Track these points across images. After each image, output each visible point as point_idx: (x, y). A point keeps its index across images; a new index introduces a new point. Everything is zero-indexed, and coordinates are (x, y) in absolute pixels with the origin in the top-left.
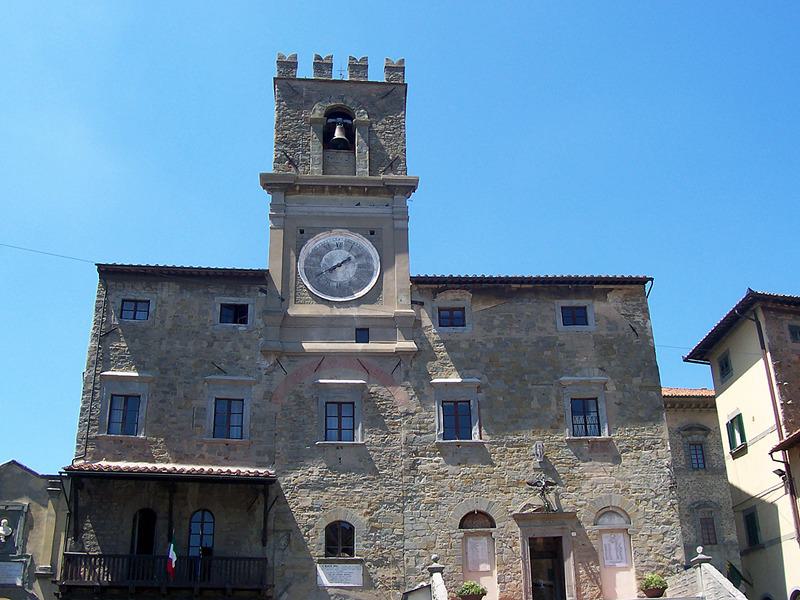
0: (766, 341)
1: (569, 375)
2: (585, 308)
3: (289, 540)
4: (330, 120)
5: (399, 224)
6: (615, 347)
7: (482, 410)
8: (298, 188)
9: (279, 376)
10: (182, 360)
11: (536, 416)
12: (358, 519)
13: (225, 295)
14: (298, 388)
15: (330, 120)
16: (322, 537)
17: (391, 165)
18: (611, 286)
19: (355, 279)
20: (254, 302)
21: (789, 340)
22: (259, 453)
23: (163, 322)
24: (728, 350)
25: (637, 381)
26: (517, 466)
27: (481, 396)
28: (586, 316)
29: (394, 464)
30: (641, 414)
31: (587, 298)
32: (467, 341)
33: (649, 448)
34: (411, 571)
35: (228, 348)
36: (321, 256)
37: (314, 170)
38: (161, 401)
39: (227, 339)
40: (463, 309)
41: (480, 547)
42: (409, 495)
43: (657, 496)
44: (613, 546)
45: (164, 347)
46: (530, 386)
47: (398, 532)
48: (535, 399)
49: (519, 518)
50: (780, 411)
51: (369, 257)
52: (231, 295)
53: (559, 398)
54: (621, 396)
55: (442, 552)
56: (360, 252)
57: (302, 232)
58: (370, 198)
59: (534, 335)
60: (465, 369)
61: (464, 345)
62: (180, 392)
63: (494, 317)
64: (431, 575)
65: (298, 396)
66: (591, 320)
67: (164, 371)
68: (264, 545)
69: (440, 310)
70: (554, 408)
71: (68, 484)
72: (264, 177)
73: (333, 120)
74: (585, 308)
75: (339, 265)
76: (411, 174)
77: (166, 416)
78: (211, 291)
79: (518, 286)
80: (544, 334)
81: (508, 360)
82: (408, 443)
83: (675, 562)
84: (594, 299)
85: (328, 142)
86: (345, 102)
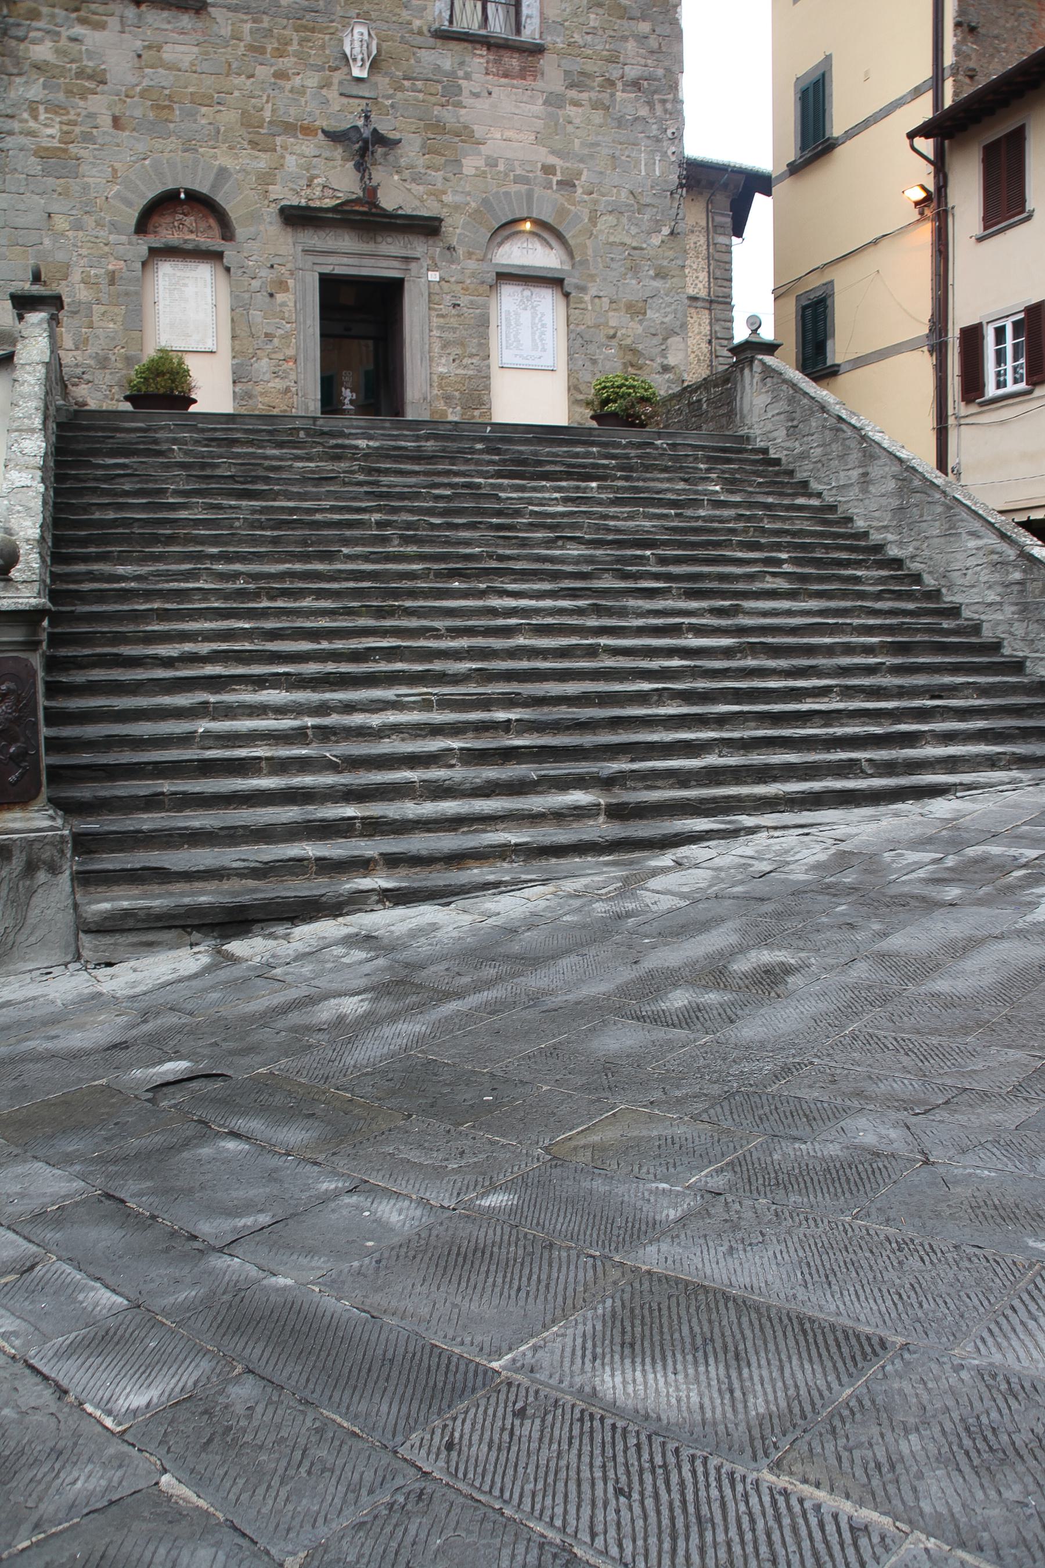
26: (297, 81)
33: (635, 85)
43: (642, 207)
49: (297, 218)
50: (950, 40)
64: (21, 318)
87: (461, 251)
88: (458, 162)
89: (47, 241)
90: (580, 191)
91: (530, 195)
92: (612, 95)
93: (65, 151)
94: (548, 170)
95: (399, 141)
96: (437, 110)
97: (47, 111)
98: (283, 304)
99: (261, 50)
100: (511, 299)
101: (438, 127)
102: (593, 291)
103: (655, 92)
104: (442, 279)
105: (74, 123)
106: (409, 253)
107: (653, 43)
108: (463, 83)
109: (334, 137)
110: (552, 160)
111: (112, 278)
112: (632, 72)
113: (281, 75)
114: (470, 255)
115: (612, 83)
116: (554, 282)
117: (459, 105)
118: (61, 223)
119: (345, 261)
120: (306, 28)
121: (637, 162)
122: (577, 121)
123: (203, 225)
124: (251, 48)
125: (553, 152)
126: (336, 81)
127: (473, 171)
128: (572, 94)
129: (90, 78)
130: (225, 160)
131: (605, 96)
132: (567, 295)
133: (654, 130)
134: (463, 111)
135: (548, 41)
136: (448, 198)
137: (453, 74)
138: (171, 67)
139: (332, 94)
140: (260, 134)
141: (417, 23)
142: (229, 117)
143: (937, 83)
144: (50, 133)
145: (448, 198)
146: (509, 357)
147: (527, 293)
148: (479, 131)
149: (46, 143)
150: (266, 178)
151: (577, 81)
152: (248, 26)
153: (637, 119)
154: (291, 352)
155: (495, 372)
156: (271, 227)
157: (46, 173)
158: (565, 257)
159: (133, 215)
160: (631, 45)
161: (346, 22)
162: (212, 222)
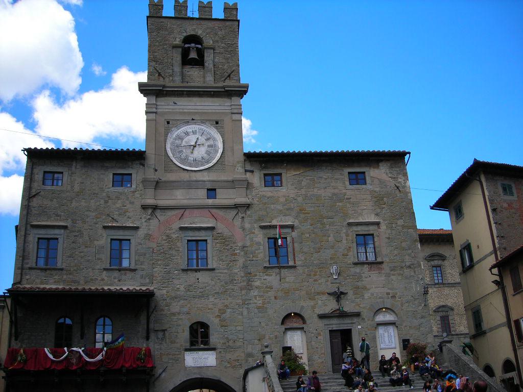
0: (487, 193)
2: (364, 173)
3: (164, 334)
4: (187, 46)
5: (235, 117)
7: (296, 245)
8: (165, 92)
9: (154, 222)
10: (86, 213)
11: (332, 247)
12: (213, 321)
13: (112, 167)
14: (168, 231)
15: (187, 46)
16: (184, 335)
17: (229, 76)
18: (382, 158)
19: (206, 155)
21: (502, 195)
22: (142, 277)
23: (72, 187)
24: (461, 201)
25: (400, 222)
27: (294, 234)
28: (365, 179)
29: (235, 282)
31: (366, 166)
32: (284, 196)
33: (409, 267)
34: (250, 355)
35: (119, 204)
36: (182, 139)
37: (175, 82)
39: (118, 198)
41: (295, 338)
42: (246, 303)
43: (415, 300)
44: (386, 335)
46: (327, 226)
47: (239, 328)
48: (331, 235)
49: (322, 317)
51: (214, 140)
52: (120, 168)
53: (347, 235)
56: (209, 136)
57: (168, 123)
59: (329, 192)
60: (283, 216)
61: (282, 200)
66: (367, 178)
67: (74, 221)
68: (148, 338)
69: (265, 175)
71: (9, 301)
74: (364, 173)
76: (243, 81)
77: (77, 253)
79: (319, 158)
80: (336, 191)
81: (313, 209)
82: (245, 267)
85: (186, 61)
87: (366, 320)
89: (259, 329)
91: (383, 302)
93: (263, 306)
94: (388, 294)
97: (259, 297)
98: (320, 339)
99: (310, 275)
100: (381, 330)
101: (357, 288)
102: (404, 325)
103: (415, 268)
105: (265, 299)
107: (413, 255)
110: (389, 291)
111: (276, 337)
112: (408, 264)
113: (315, 280)
114: (369, 320)
115: (402, 267)
116: (392, 324)
117: (362, 281)
118: (263, 324)
120: (321, 268)
121: (413, 287)
122: (394, 279)
123: (298, 320)
124: (307, 275)
126: (329, 280)
127: (367, 298)
128: (392, 272)
129: (269, 288)
130: (302, 303)
131: (401, 272)
132: (397, 327)
134: (363, 282)
137: (360, 273)
138: (288, 283)
139: (329, 283)
140: (311, 296)
141: (349, 262)
142: (304, 293)
143: (495, 251)
144: (259, 302)
146: (382, 346)
148: (368, 287)
149: (259, 305)
150: (313, 307)
152: (306, 270)
155: (379, 350)
156: (316, 319)
157: (260, 312)
158: (395, 316)
160: (407, 257)
162: (300, 319)
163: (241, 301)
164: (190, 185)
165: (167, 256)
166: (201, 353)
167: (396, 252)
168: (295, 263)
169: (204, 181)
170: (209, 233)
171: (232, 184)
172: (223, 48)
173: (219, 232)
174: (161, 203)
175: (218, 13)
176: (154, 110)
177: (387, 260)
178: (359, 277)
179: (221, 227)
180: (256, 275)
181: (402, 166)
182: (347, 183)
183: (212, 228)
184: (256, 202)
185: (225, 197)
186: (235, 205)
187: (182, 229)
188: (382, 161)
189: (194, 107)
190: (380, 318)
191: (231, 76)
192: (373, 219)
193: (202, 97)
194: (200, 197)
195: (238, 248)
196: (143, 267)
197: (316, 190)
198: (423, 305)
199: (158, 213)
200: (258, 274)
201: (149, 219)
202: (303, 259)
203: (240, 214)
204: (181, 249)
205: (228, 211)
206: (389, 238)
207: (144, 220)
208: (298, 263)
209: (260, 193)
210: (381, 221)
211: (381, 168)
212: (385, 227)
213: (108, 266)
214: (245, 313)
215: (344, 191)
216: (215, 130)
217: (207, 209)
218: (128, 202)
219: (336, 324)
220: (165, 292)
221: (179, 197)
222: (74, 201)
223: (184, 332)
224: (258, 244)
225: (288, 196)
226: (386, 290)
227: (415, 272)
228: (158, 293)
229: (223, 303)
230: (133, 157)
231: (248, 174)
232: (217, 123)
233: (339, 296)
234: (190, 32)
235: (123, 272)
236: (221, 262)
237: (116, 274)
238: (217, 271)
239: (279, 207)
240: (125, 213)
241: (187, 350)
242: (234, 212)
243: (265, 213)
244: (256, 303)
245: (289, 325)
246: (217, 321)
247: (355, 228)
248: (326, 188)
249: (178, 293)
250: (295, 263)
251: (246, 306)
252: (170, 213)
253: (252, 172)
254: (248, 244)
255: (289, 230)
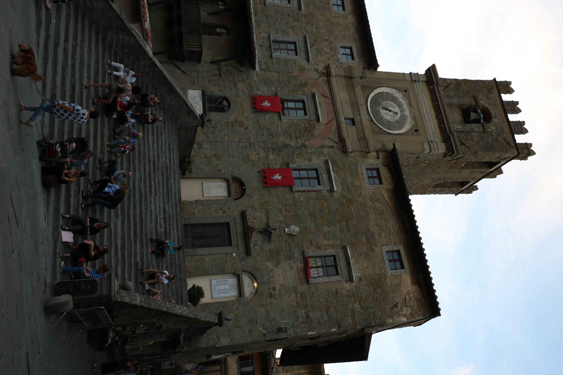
1: (352, 253)
2: (402, 267)
3: (216, 75)
4: (479, 111)
6: (379, 290)
7: (314, 193)
8: (432, 87)
9: (315, 75)
12: (231, 116)
13: (357, 47)
14: (309, 85)
17: (464, 144)
20: (357, 65)
22: (266, 63)
23: (334, 17)
26: (280, 215)
30: (331, 309)
34: (200, 146)
38: (288, 14)
39: (331, 49)
40: (381, 183)
41: (219, 190)
44: (227, 287)
45: (320, 17)
46: (338, 225)
47: (226, 138)
48: (330, 229)
49: (243, 215)
52: (357, 52)
54: (344, 294)
55: (214, 164)
57: (406, 91)
58: (438, 130)
61: (357, 183)
62: (295, 24)
63: (380, 203)
65: (305, 85)
67: (306, 16)
68: (212, 62)
69: (377, 170)
70: (325, 242)
72: (433, 67)
73: (480, 112)
75: (390, 111)
78: (358, 42)
80: (377, 237)
81: (353, 211)
82: (286, 146)
83: (218, 337)
84: (411, 274)
86: (494, 118)
88: (269, 261)
90: (270, 300)
92: (302, 309)
94: (274, 289)
95: (270, 242)
96: (282, 254)
101: (278, 254)
104: (234, 257)
106: (240, 247)
108: (292, 261)
109: (268, 224)
112: (311, 314)
115: (306, 308)
117: (286, 260)
118: (231, 159)
119: (234, 229)
124: (285, 203)
125: (280, 291)
128: (299, 296)
133: (296, 324)
135: (312, 286)
136: (258, 257)
141: (305, 246)
144: (253, 157)
145: (258, 257)
147: (235, 287)
151: (302, 295)
153: (297, 318)
154: (206, 215)
159: (236, 175)
161: (299, 227)
163: (253, 141)
164: (354, 104)
165: (287, 83)
166: (201, 103)
167: (322, 300)
168: (296, 191)
169: (360, 115)
170: (313, 117)
171: (363, 139)
172: (488, 141)
173: (316, 127)
174: (333, 80)
175: (520, 139)
176: (414, 79)
177: (312, 290)
178: (289, 257)
179: (319, 129)
180: (279, 156)
181: (421, 313)
182: (385, 248)
183: (318, 120)
184: (350, 159)
185: (349, 132)
186: (344, 139)
187: (314, 95)
188: (421, 288)
189: (425, 112)
190: (246, 280)
191: (464, 146)
192: (355, 275)
193: (436, 119)
194: (346, 111)
195: (303, 141)
196: (275, 64)
197: (373, 215)
198: (265, 332)
199: (324, 78)
200: (281, 158)
201: (317, 71)
202: (302, 199)
203: (336, 144)
204: (295, 94)
205: (337, 135)
206: (337, 292)
207: (316, 67)
208: (297, 195)
209: (359, 165)
210: (354, 284)
211: (413, 288)
212: (348, 288)
213: (272, 38)
214: (242, 144)
215: (378, 244)
216: (409, 128)
217: (334, 117)
218: (329, 56)
219: (236, 229)
220: (255, 79)
221: (341, 95)
222: (323, 17)
223: (220, 91)
224: (310, 160)
225: (361, 189)
226: (278, 287)
227: (303, 323)
228: (253, 73)
229: (249, 125)
230: (370, 59)
231: (375, 154)
232: (416, 131)
233: (267, 232)
234: (493, 112)
235: (268, 49)
236: (287, 126)
237: (266, 43)
238: (279, 122)
239: (349, 180)
240: (320, 54)
241: (203, 93)
242: (336, 139)
243: (341, 166)
244: (252, 154)
245: (234, 187)
246: (232, 119)
247: (341, 255)
248: (378, 226)
249: (255, 89)
250: (296, 191)
251: (248, 146)
252: (326, 88)
253: (378, 158)
254: (309, 150)
255: (328, 188)
